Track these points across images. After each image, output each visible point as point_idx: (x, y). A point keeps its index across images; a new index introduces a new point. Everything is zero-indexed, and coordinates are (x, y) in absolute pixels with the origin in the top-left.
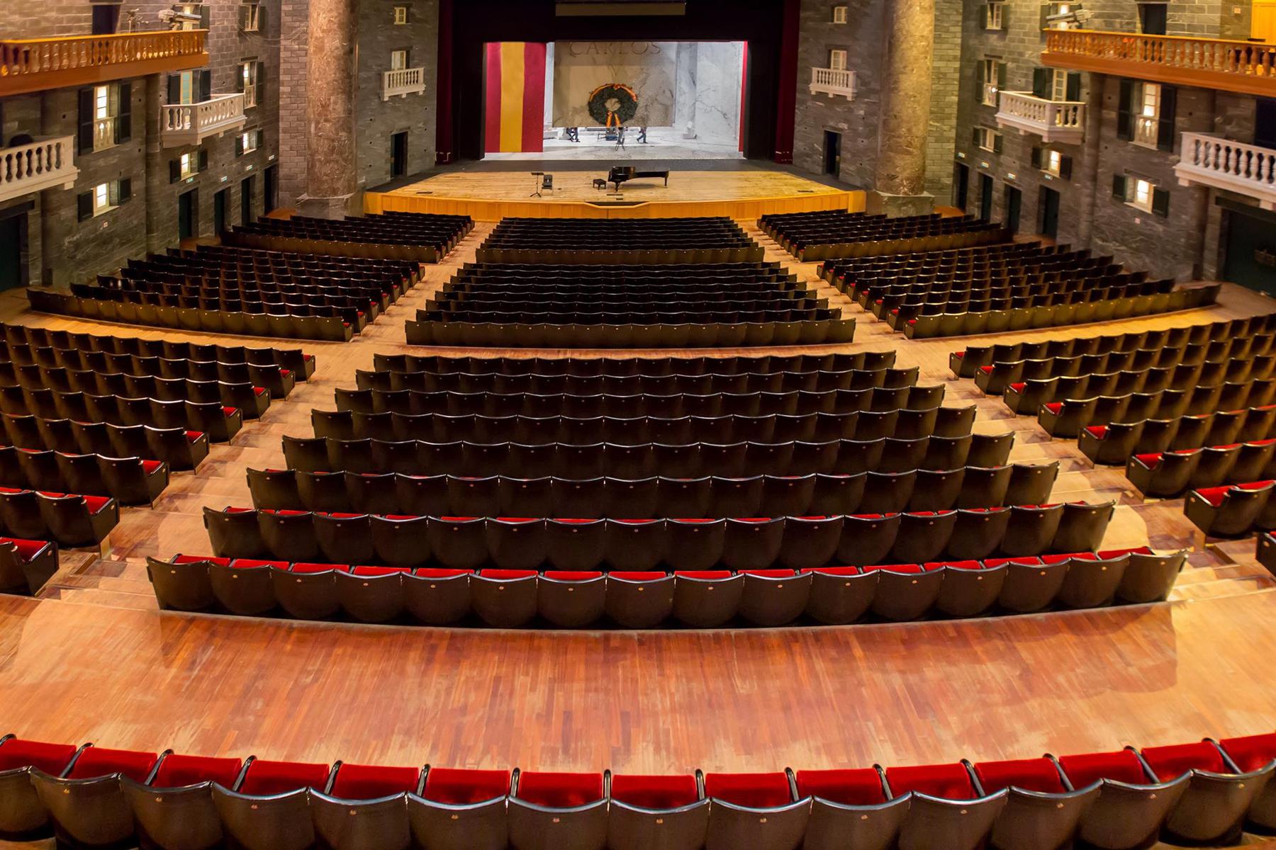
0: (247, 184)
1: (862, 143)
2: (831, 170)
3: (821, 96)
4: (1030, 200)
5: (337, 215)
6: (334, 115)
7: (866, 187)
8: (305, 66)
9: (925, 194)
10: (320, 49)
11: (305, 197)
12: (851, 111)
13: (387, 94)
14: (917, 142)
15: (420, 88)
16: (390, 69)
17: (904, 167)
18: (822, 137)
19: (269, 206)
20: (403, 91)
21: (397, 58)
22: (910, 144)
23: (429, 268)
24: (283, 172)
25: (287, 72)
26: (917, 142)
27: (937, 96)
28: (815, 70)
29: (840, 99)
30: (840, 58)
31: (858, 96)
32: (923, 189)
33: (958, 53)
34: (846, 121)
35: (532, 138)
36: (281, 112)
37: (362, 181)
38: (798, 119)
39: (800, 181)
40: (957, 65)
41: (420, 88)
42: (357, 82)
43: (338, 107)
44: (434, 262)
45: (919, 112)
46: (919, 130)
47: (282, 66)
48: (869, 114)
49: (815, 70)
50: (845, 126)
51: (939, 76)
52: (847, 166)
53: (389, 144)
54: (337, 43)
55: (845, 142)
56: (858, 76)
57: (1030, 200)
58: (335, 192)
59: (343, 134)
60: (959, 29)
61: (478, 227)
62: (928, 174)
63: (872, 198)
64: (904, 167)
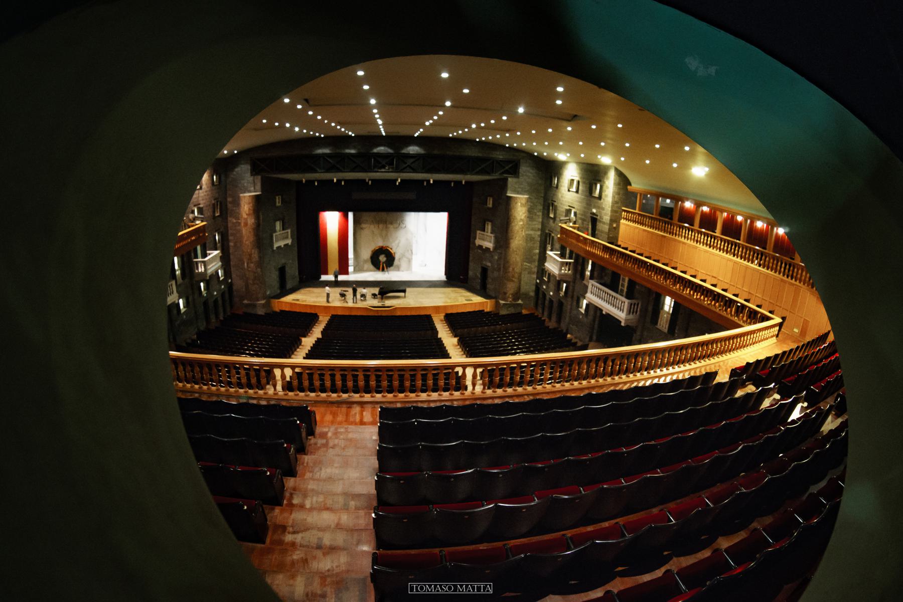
0: (223, 295)
1: (496, 274)
2: (482, 291)
3: (480, 247)
4: (555, 305)
5: (261, 312)
6: (254, 260)
7: (495, 298)
8: (240, 231)
9: (520, 302)
10: (246, 224)
11: (246, 302)
12: (492, 257)
13: (276, 246)
14: (516, 275)
15: (289, 241)
16: (275, 231)
17: (511, 288)
18: (480, 270)
19: (232, 306)
20: (281, 244)
21: (278, 225)
22: (513, 277)
23: (303, 339)
24: (235, 288)
25: (232, 235)
26: (516, 275)
27: (529, 250)
28: (478, 232)
29: (487, 249)
30: (489, 227)
31: (495, 248)
32: (518, 300)
33: (540, 227)
34: (490, 262)
35: (344, 270)
36: (232, 257)
37: (268, 293)
38: (471, 258)
39: (469, 294)
40: (539, 233)
41: (289, 241)
42: (262, 238)
43: (256, 256)
44: (305, 336)
45: (518, 259)
46: (517, 270)
47: (230, 232)
48: (500, 258)
49: (478, 232)
50: (489, 264)
51: (529, 239)
52: (490, 286)
53: (277, 273)
54: (253, 220)
55: (490, 274)
56: (495, 237)
57: (555, 305)
58: (258, 300)
59: (259, 270)
60: (540, 214)
61: (321, 318)
62: (523, 290)
63: (497, 304)
64: (511, 288)
